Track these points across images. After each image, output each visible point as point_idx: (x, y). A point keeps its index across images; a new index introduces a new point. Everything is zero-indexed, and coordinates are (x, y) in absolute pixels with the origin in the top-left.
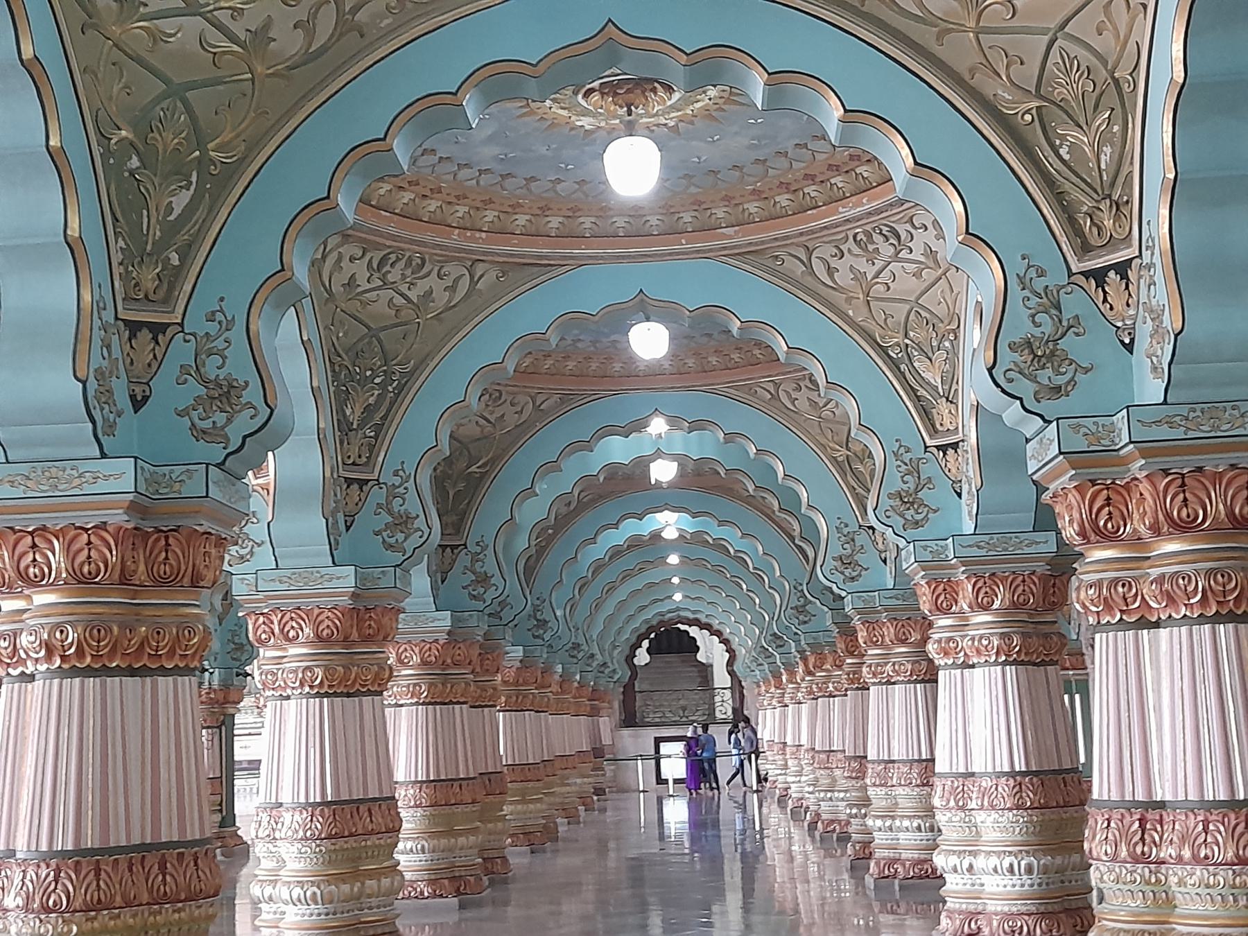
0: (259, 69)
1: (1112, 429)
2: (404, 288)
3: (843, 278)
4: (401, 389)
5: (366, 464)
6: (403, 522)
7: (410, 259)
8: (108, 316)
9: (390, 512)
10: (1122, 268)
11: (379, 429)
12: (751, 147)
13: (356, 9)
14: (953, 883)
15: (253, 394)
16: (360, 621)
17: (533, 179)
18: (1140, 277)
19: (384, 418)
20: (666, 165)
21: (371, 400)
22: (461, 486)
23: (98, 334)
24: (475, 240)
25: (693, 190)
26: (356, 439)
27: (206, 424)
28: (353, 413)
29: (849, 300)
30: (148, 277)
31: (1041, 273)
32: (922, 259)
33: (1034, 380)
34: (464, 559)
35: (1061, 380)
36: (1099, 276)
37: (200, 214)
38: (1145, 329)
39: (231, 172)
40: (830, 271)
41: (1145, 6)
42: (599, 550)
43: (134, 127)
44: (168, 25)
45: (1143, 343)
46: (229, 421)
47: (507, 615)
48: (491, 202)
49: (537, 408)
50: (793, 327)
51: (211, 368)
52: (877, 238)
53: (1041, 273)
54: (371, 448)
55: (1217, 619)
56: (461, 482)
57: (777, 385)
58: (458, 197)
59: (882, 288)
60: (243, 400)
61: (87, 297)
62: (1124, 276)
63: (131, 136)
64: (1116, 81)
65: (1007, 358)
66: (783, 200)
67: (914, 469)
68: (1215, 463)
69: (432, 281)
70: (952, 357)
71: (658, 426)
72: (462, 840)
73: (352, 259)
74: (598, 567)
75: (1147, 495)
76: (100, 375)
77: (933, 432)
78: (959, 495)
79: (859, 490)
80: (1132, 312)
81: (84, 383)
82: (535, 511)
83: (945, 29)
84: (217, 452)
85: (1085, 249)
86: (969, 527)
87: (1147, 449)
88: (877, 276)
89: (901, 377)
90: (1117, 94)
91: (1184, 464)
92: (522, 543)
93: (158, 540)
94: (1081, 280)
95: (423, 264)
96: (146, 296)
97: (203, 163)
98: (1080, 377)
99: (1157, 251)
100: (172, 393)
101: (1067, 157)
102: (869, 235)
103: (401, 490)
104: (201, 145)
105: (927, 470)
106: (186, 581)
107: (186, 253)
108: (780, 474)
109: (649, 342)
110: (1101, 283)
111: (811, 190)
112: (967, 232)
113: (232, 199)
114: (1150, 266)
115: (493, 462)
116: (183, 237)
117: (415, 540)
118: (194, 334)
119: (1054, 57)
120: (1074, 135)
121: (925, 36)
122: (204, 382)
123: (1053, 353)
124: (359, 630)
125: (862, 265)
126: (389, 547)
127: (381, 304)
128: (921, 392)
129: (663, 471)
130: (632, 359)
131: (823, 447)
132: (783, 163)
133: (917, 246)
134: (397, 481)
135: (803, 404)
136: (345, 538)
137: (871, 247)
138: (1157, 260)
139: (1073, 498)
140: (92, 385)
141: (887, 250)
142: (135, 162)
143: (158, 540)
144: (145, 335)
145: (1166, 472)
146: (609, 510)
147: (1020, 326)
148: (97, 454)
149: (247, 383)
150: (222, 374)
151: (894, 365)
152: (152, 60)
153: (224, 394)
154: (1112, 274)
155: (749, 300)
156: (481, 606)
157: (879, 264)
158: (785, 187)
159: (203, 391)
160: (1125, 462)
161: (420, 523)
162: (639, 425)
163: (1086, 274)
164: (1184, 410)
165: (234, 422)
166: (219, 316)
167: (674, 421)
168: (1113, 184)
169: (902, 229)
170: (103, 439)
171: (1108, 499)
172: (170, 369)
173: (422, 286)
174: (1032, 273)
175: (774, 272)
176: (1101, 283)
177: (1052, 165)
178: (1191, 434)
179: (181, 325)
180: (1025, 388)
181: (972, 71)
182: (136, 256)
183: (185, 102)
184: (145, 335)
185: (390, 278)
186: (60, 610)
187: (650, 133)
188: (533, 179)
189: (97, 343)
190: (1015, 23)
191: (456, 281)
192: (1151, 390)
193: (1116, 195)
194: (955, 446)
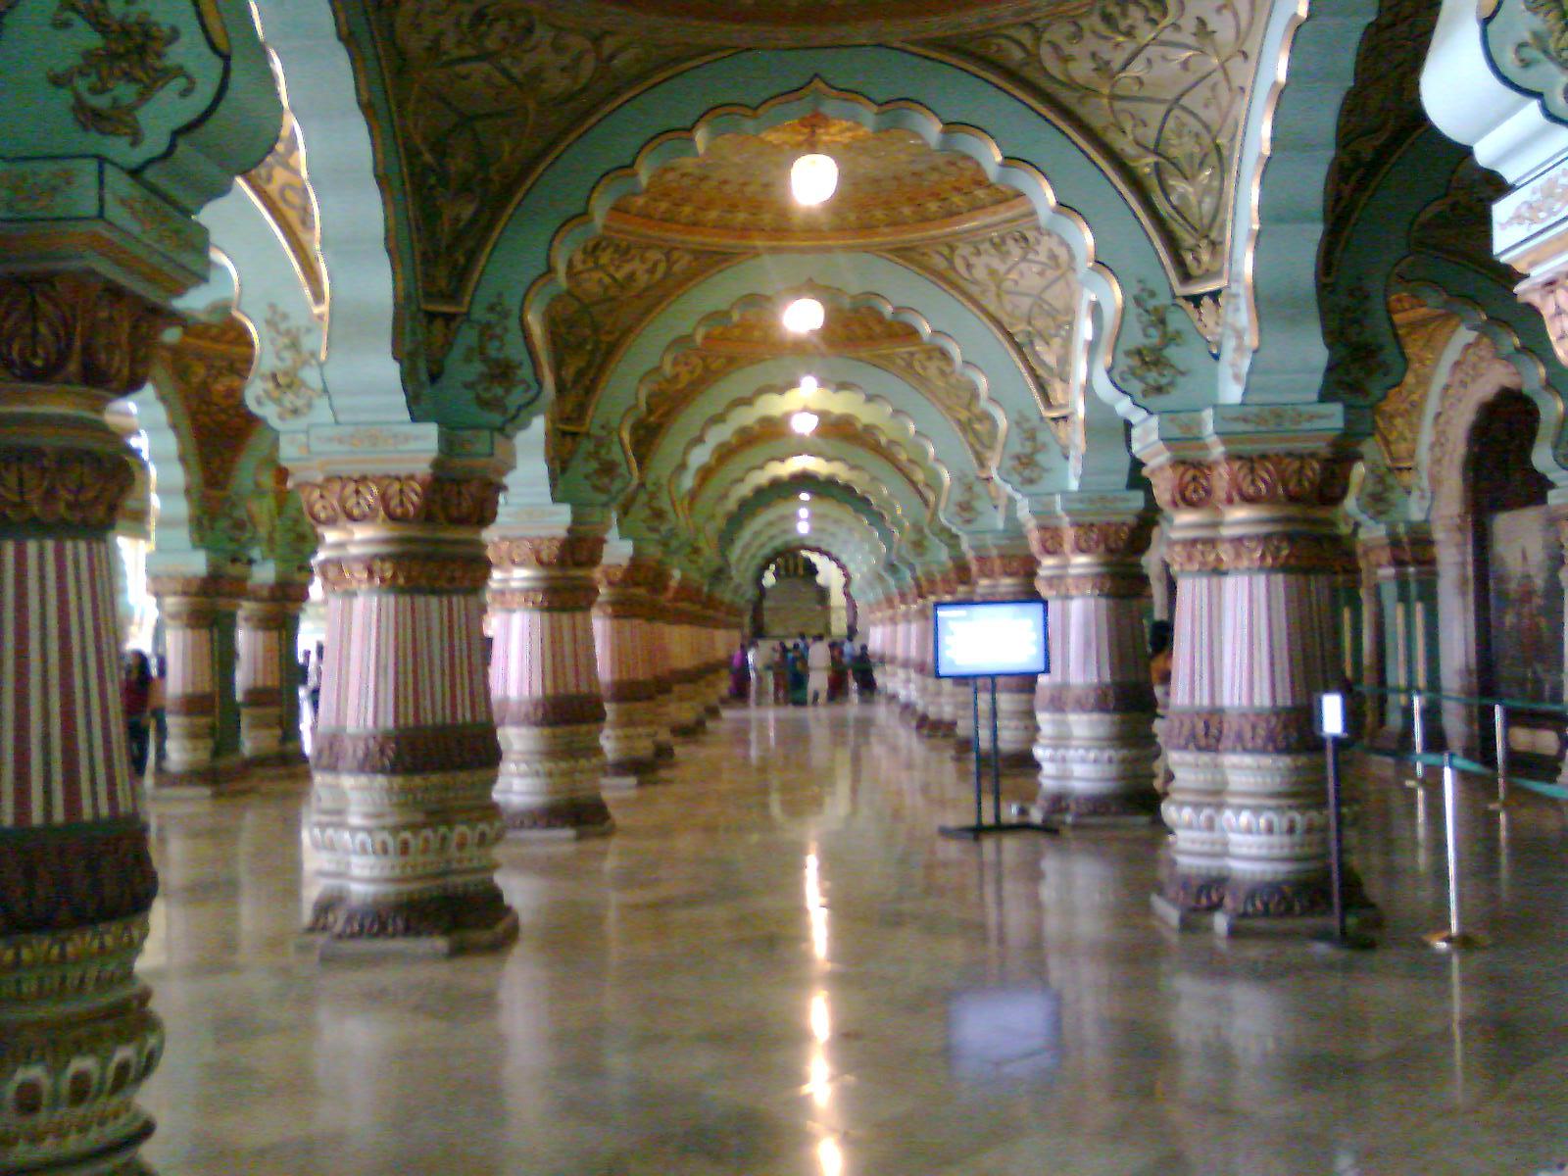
1: (1199, 424)
2: (612, 269)
3: (980, 273)
8: (414, 308)
10: (1214, 295)
13: (612, 57)
14: (1048, 768)
17: (725, 182)
20: (842, 177)
29: (984, 292)
33: (1142, 379)
35: (1163, 381)
36: (1196, 300)
38: (1229, 345)
39: (509, 190)
40: (969, 266)
43: (432, 150)
44: (462, 69)
45: (1228, 354)
47: (674, 544)
50: (933, 314)
51: (492, 350)
52: (1010, 243)
53: (1152, 294)
55: (1272, 570)
57: (912, 354)
62: (1216, 301)
64: (1218, 148)
65: (1124, 362)
66: (933, 206)
67: (1031, 436)
69: (636, 264)
70: (1068, 340)
72: (640, 730)
77: (1048, 404)
78: (1067, 458)
79: (978, 447)
82: (700, 456)
83: (1088, 91)
86: (1074, 485)
87: (1225, 436)
88: (1009, 271)
89: (1025, 361)
90: (1219, 157)
94: (1182, 302)
100: (462, 369)
101: (1175, 203)
105: (1042, 436)
111: (957, 199)
115: (668, 414)
117: (617, 485)
119: (1171, 124)
120: (1179, 186)
121: (1068, 97)
122: (485, 358)
126: (595, 488)
128: (1040, 371)
129: (804, 425)
131: (948, 409)
132: (935, 176)
138: (1242, 292)
139: (1169, 473)
141: (1016, 250)
147: (1135, 338)
149: (521, 364)
150: (501, 356)
151: (1018, 348)
155: (899, 290)
156: (655, 536)
157: (1010, 262)
161: (623, 470)
162: (793, 384)
163: (1187, 298)
166: (499, 308)
168: (1211, 226)
169: (1030, 235)
173: (627, 268)
174: (1145, 295)
177: (1164, 208)
179: (468, 314)
180: (1136, 387)
181: (1105, 129)
188: (725, 182)
190: (1144, 93)
191: (656, 264)
193: (1211, 234)
194: (1065, 418)
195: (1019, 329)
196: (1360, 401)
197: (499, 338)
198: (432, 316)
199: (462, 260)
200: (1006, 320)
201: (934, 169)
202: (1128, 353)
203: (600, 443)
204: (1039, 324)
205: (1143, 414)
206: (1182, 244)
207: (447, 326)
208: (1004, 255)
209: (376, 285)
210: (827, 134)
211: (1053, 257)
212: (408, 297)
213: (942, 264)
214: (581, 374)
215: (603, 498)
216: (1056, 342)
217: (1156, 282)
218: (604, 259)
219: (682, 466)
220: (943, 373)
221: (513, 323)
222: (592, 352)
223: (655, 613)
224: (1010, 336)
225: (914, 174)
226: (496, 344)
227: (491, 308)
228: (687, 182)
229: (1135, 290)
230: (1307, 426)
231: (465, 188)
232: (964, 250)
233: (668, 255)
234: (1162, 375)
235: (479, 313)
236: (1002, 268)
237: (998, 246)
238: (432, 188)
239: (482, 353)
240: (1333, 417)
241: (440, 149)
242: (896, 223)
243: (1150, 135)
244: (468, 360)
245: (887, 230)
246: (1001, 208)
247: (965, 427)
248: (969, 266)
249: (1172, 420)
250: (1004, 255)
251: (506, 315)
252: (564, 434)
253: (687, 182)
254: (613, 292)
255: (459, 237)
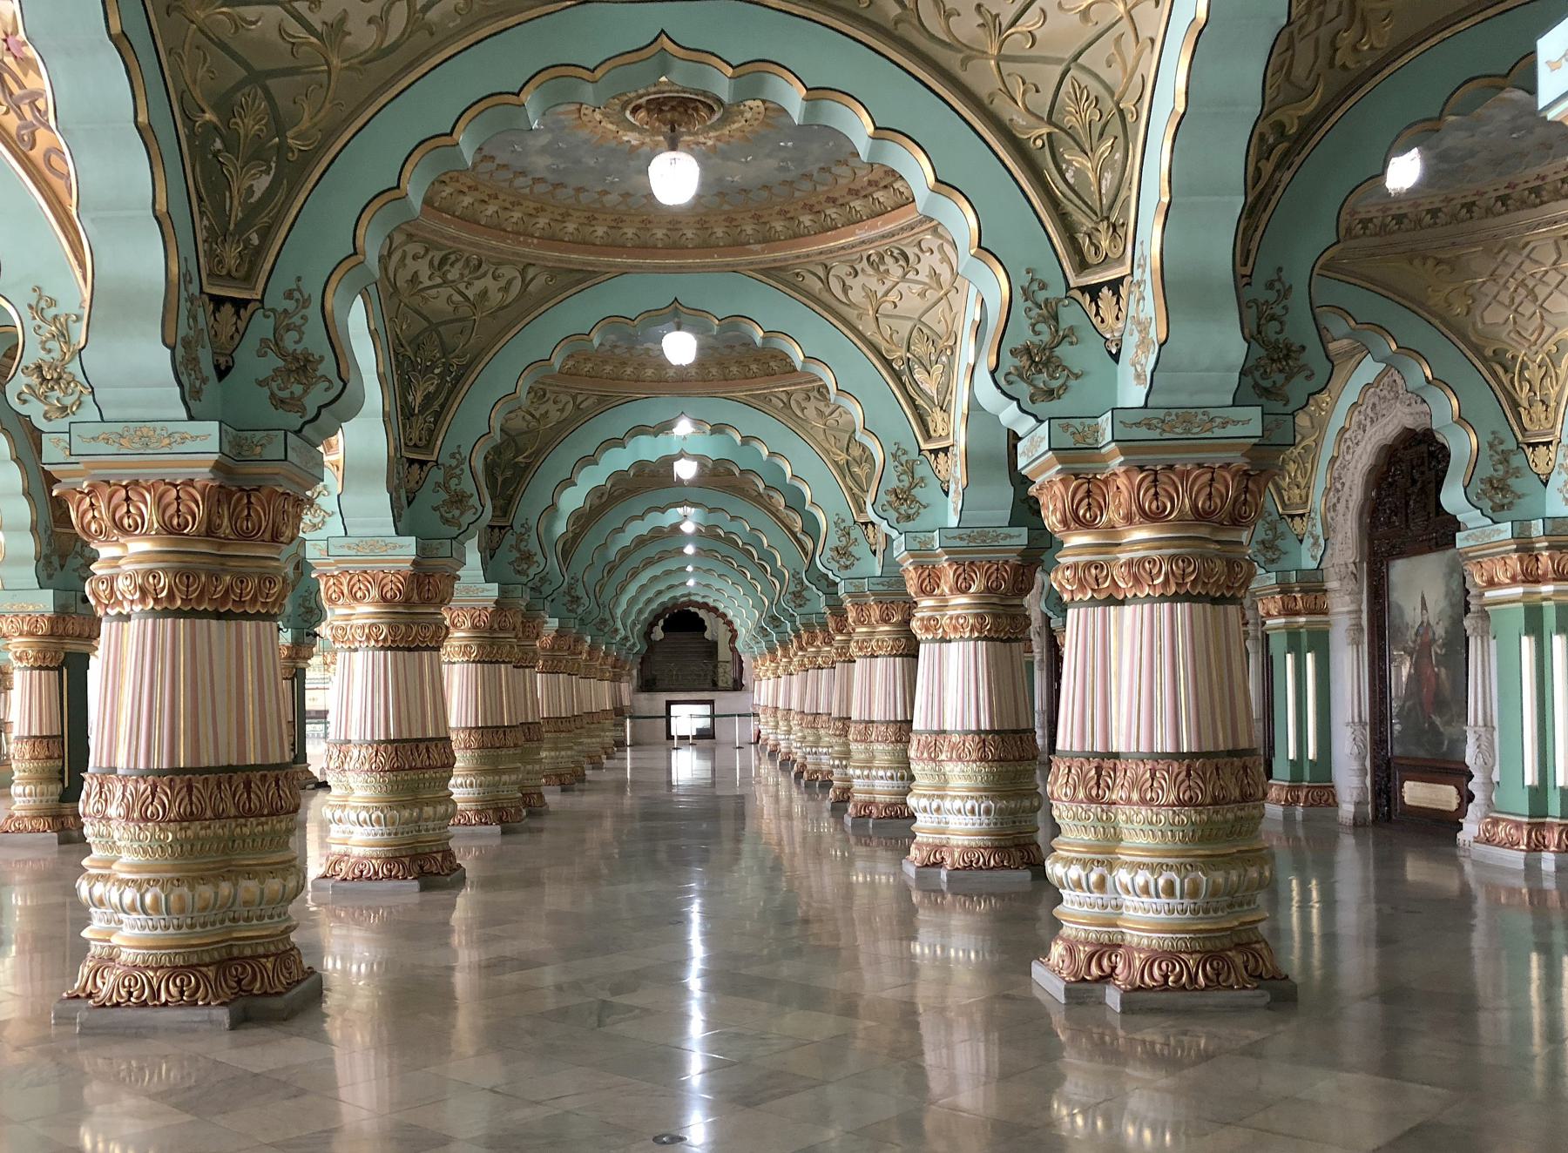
0: (335, 61)
2: (462, 286)
3: (856, 295)
4: (458, 380)
5: (426, 446)
6: (459, 500)
7: (468, 261)
8: (194, 288)
9: (447, 489)
10: (1115, 285)
11: (438, 416)
12: (781, 169)
15: (328, 367)
16: (420, 585)
18: (1130, 293)
19: (442, 406)
20: (704, 184)
21: (432, 389)
22: (509, 473)
23: (184, 305)
24: (528, 246)
25: (726, 207)
26: (419, 424)
27: (285, 394)
28: (416, 399)
29: (860, 317)
30: (231, 255)
31: (1043, 287)
32: (927, 280)
33: (1031, 383)
34: (510, 539)
35: (1055, 384)
36: (1093, 291)
37: (280, 197)
39: (308, 159)
41: (1153, 41)
42: (626, 539)
43: (216, 108)
46: (305, 391)
47: (547, 589)
48: (543, 210)
49: (577, 407)
52: (888, 259)
53: (1043, 287)
54: (431, 432)
56: (511, 469)
57: (789, 395)
58: (513, 204)
59: (890, 306)
60: (318, 374)
61: (174, 269)
62: (1116, 293)
63: (214, 119)
65: (1009, 363)
68: (1184, 461)
69: (488, 282)
70: (949, 369)
71: (684, 427)
73: (415, 257)
74: (625, 553)
75: (1123, 488)
76: (187, 343)
77: (928, 437)
80: (1120, 325)
81: (173, 349)
82: (572, 500)
84: (295, 420)
85: (1083, 266)
87: (1126, 446)
88: (886, 294)
89: (902, 386)
91: (1157, 460)
92: (561, 527)
93: (240, 499)
94: (1077, 294)
95: (480, 265)
96: (229, 274)
97: (282, 149)
98: (1072, 382)
99: (1148, 270)
100: (253, 363)
102: (882, 258)
103: (458, 471)
104: (281, 132)
106: (267, 536)
107: (266, 233)
108: (789, 475)
109: (680, 348)
110: (1095, 299)
111: (831, 211)
112: (979, 246)
113: (309, 185)
114: (1139, 284)
116: (263, 220)
117: (469, 517)
118: (273, 310)
122: (282, 354)
123: (1049, 359)
124: (419, 594)
125: (873, 283)
126: (446, 521)
127: (440, 301)
128: (919, 401)
129: (686, 470)
130: (663, 364)
131: (827, 452)
132: (807, 186)
133: (924, 268)
134: (454, 463)
135: (811, 412)
136: (406, 512)
137: (882, 268)
139: (1058, 488)
140: (180, 350)
141: (896, 271)
142: (218, 145)
143: (240, 499)
144: (228, 309)
145: (1141, 469)
146: (637, 505)
147: (1022, 334)
148: (184, 415)
149: (322, 358)
150: (299, 348)
151: (897, 375)
152: (233, 45)
153: (302, 367)
154: (1105, 290)
156: (524, 579)
157: (889, 284)
158: (809, 208)
159: (281, 363)
160: (1104, 459)
161: (474, 501)
162: (666, 427)
163: (1083, 289)
164: (1161, 414)
165: (308, 394)
167: (698, 422)
170: (191, 403)
171: (1089, 491)
172: (251, 341)
173: (479, 285)
174: (1035, 287)
175: (795, 288)
176: (1095, 299)
178: (1166, 436)
179: (262, 301)
180: (1023, 390)
182: (218, 234)
183: (266, 91)
184: (228, 309)
185: (450, 277)
186: (141, 557)
187: (690, 151)
189: (184, 313)
191: (510, 283)
192: (1133, 394)
195: (896, 355)
196: (1277, 407)
197: (299, 329)
198: (218, 301)
199: (255, 241)
200: (883, 346)
201: (807, 176)
202: (1013, 352)
203: (450, 473)
204: (919, 349)
205: (1032, 421)
206: (1079, 227)
207: (237, 313)
208: (883, 276)
209: (144, 260)
210: (690, 133)
211: (935, 275)
212: (185, 278)
213: (817, 286)
214: (428, 398)
215: (455, 531)
216: (937, 369)
217: (1051, 274)
218: (453, 274)
219: (553, 507)
220: (820, 413)
221: (314, 311)
222: (441, 376)
223: (524, 663)
224: (888, 363)
225: (785, 182)
226: (294, 335)
227: (289, 295)
228: (540, 188)
229: (1025, 280)
230: (1218, 432)
231: (257, 156)
232: (841, 269)
233: (523, 273)
234: (1053, 378)
235: (275, 300)
236: (881, 291)
237: (876, 264)
238: (216, 154)
239: (277, 344)
240: (1250, 422)
241: (226, 106)
242: (767, 240)
243: (1043, 102)
244: (262, 355)
245: (758, 247)
246: (879, 221)
247: (844, 470)
248: (845, 288)
249: (1066, 428)
250: (883, 276)
251: (306, 303)
252: (411, 462)
253: (540, 188)
254: (465, 310)
255: (252, 211)
